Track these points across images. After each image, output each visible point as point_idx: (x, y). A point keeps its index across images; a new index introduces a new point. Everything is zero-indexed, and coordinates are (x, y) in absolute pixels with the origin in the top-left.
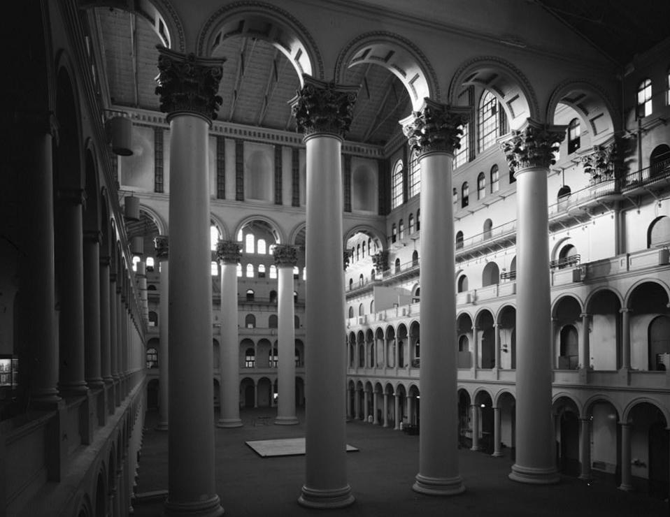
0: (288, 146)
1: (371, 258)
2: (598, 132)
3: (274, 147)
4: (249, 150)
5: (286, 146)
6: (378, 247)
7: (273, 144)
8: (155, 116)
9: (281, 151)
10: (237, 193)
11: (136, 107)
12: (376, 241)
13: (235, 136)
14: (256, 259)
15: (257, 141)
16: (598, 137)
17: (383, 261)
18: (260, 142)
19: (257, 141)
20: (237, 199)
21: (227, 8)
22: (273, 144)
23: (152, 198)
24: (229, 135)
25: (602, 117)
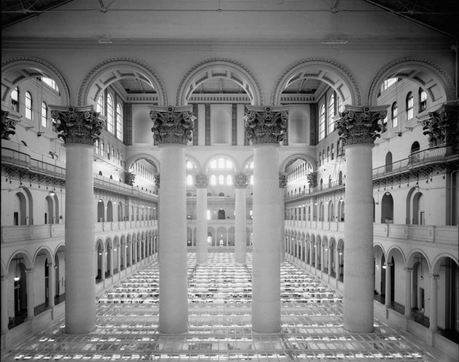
0: (242, 104)
1: (306, 176)
2: (436, 99)
3: (231, 105)
4: (214, 111)
5: (240, 104)
7: (231, 104)
8: (154, 96)
9: (236, 108)
10: (206, 140)
11: (143, 93)
12: (309, 164)
13: (205, 102)
15: (220, 103)
16: (435, 103)
17: (314, 179)
18: (222, 103)
19: (220, 103)
20: (206, 145)
21: (103, 64)
22: (231, 104)
23: (152, 149)
24: (200, 102)
25: (436, 86)
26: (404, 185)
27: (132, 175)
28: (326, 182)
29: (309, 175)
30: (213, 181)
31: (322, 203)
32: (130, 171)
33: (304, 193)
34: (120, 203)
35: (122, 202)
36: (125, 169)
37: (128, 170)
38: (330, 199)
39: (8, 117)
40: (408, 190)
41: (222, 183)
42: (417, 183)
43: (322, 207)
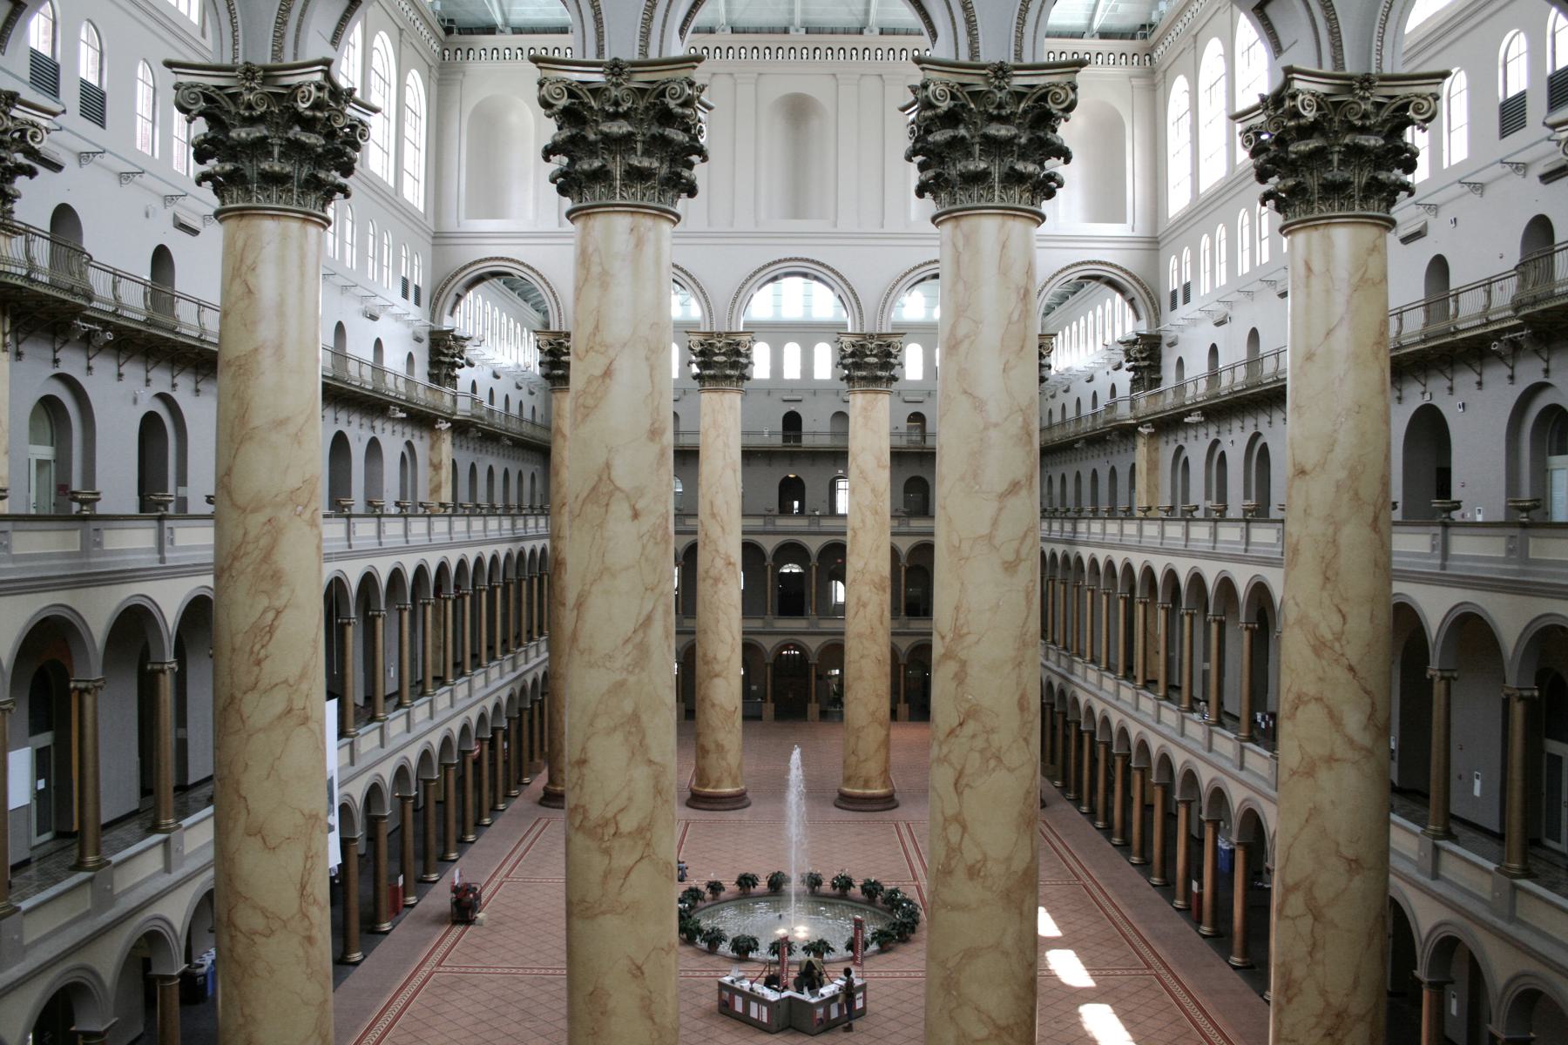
6: (1138, 317)
26: (1496, 375)
27: (456, 338)
28: (1197, 366)
29: (1135, 342)
30: (761, 368)
31: (1180, 449)
32: (447, 323)
33: (1111, 407)
34: (409, 444)
35: (416, 443)
36: (432, 320)
37: (441, 322)
38: (1213, 436)
39: (14, 113)
40: (1514, 393)
41: (792, 371)
42: (1547, 371)
43: (1181, 463)
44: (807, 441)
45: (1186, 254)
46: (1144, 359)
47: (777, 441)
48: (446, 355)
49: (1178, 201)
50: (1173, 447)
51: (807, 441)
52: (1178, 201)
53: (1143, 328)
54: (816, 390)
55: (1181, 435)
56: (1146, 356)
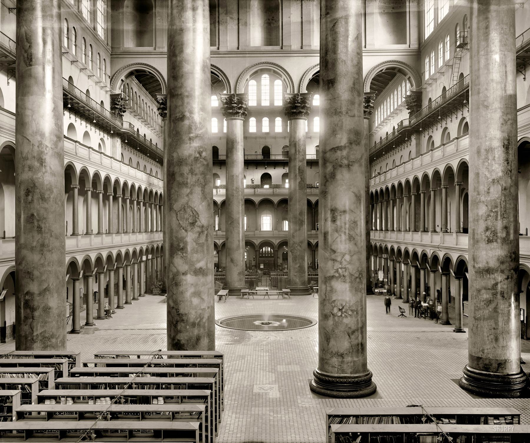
6: (412, 86)
14: (271, 113)
29: (410, 96)
31: (431, 137)
38: (444, 126)
41: (266, 129)
44: (273, 158)
45: (433, 55)
46: (414, 102)
47: (260, 157)
48: (118, 105)
49: (429, 30)
50: (427, 137)
51: (273, 158)
52: (429, 30)
53: (414, 89)
54: (276, 137)
55: (431, 130)
56: (415, 102)
